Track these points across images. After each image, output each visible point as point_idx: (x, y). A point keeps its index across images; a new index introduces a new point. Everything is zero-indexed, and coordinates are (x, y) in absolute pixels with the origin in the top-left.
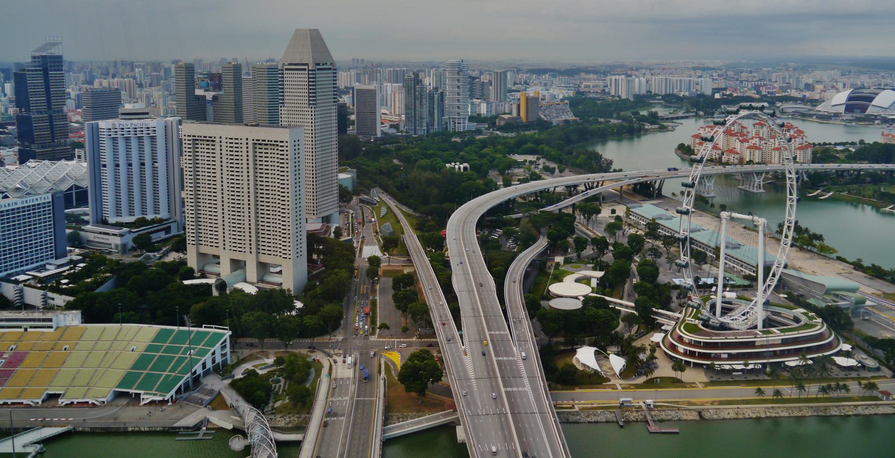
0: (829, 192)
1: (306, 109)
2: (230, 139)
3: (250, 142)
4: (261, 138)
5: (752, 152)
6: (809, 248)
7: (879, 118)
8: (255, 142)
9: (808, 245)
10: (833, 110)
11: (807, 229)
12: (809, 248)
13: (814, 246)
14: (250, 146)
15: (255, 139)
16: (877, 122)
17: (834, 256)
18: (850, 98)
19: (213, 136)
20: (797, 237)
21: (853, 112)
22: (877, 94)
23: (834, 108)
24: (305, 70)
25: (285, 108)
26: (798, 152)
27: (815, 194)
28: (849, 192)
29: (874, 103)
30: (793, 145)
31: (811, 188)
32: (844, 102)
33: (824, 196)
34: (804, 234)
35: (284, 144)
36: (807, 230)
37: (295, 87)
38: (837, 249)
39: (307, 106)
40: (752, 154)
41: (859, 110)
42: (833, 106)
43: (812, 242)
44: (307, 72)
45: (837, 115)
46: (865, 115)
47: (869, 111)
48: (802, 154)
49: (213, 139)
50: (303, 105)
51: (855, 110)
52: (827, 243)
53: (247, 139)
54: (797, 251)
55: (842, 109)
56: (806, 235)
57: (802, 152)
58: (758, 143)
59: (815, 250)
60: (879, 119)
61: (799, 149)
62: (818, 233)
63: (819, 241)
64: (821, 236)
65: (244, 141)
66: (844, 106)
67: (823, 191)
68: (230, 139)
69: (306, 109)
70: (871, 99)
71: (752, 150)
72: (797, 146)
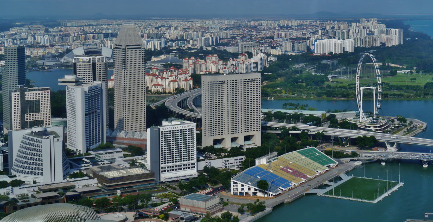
1: (140, 71)
2: (233, 81)
3: (242, 81)
4: (248, 79)
5: (174, 83)
8: (245, 80)
14: (243, 83)
15: (245, 79)
19: (224, 80)
24: (140, 48)
25: (127, 71)
26: (184, 82)
35: (237, 81)
37: (134, 58)
39: (141, 69)
40: (174, 84)
44: (141, 49)
48: (186, 83)
49: (224, 82)
50: (139, 69)
53: (241, 80)
57: (186, 82)
58: (175, 78)
65: (240, 81)
68: (233, 81)
69: (140, 71)
71: (174, 82)
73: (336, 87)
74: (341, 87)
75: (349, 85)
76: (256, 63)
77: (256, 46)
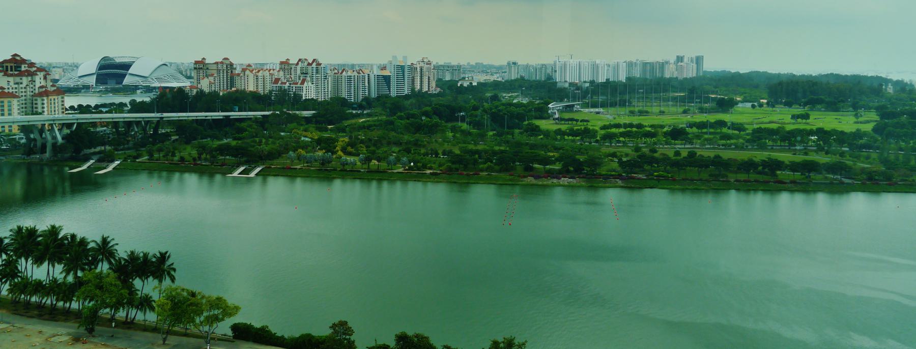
0: (112, 161)
6: (121, 314)
7: (140, 87)
9: (116, 306)
10: (81, 82)
11: (105, 241)
12: (121, 314)
13: (145, 303)
16: (138, 91)
17: (224, 328)
18: (101, 67)
20: (70, 279)
21: (107, 84)
22: (134, 62)
23: (82, 80)
27: (85, 167)
28: (151, 155)
29: (130, 71)
30: (28, 89)
31: (72, 159)
32: (94, 72)
33: (105, 168)
34: (95, 262)
36: (105, 249)
38: (231, 301)
41: (114, 81)
42: (80, 77)
43: (132, 291)
45: (87, 88)
46: (123, 85)
47: (128, 80)
51: (109, 81)
52: (184, 281)
54: (76, 339)
55: (92, 81)
56: (104, 267)
59: (151, 317)
60: (141, 88)
61: (41, 95)
62: (152, 249)
63: (160, 279)
64: (163, 257)
66: (95, 77)
67: (99, 161)
70: (127, 66)
72: (37, 91)
73: (559, 132)
74: (573, 133)
75: (604, 128)
76: (387, 79)
77: (456, 70)
